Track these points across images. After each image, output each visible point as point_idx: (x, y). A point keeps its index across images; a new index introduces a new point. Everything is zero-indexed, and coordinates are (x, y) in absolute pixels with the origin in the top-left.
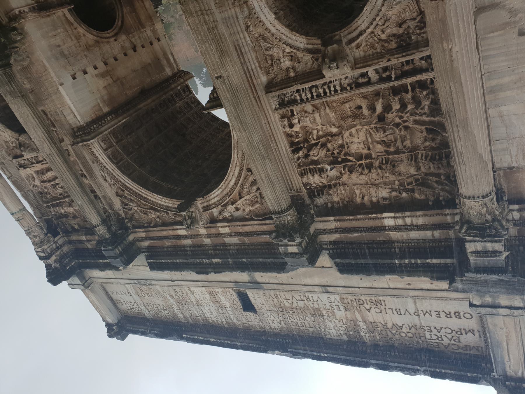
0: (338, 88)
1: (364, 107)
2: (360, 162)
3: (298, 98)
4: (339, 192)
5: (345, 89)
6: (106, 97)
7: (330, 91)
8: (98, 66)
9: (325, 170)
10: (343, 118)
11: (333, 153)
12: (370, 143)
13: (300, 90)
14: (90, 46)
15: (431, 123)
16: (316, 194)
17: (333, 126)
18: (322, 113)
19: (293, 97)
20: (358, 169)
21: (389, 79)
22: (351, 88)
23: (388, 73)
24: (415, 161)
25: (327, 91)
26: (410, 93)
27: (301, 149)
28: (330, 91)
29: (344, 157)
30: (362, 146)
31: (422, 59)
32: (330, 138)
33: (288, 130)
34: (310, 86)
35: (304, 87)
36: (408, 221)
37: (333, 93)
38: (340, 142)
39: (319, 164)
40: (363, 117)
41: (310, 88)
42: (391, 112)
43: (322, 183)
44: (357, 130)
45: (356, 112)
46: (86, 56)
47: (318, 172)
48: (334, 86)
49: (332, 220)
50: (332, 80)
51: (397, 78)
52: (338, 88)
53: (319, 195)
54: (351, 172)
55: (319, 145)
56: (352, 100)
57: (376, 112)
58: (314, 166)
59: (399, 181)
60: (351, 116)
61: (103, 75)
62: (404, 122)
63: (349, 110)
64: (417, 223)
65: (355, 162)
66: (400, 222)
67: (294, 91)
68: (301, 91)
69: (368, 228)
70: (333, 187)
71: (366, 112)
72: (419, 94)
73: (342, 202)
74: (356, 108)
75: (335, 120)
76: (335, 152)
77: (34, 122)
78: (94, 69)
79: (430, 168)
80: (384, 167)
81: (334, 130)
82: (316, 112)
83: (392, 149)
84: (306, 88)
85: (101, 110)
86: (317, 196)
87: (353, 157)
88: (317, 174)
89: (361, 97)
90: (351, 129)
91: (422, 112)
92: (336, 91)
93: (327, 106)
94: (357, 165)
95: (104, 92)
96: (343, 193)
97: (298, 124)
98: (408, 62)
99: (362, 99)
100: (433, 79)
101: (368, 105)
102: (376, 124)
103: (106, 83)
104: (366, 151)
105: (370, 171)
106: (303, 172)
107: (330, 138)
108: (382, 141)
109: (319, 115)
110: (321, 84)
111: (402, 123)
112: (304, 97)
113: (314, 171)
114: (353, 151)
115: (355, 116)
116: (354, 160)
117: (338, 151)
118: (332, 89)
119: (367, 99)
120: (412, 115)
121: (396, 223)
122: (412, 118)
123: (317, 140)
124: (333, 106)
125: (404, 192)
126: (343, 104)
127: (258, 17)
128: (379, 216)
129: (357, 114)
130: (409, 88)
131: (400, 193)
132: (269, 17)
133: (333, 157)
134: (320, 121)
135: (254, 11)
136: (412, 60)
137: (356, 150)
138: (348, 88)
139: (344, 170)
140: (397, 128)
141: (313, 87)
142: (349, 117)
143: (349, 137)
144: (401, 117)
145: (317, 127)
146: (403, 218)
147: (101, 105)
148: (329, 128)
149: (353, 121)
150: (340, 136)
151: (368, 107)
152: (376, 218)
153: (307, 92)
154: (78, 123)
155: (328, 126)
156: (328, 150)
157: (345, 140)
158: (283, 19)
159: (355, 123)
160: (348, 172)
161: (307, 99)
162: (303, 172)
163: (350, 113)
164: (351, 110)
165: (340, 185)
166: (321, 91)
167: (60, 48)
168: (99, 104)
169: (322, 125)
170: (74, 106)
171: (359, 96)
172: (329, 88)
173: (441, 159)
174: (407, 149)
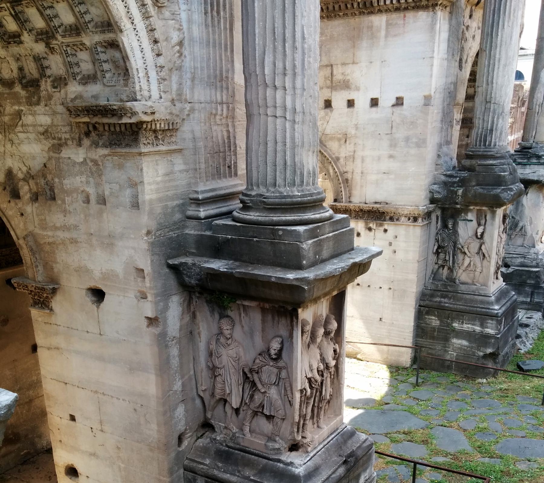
6: (365, 44)
8: (345, 104)
14: (339, 140)
46: (357, 127)
61: (346, 85)
77: (503, 52)
78: (356, 102)
85: (388, 24)
95: (363, 54)
103: (348, 69)
127: (158, 55)
132: (135, 44)
135: (163, 74)
147: (383, 33)
154: (442, 18)
158: (92, 24)
167: (391, 152)
168: (386, 36)
170: (433, 51)
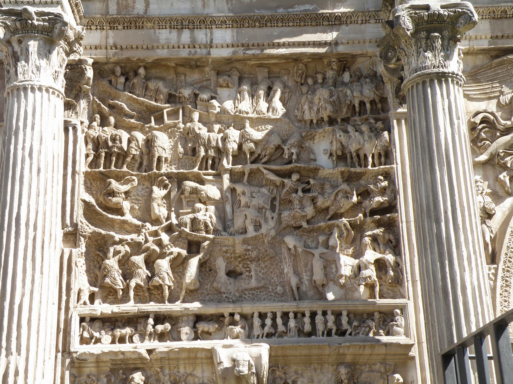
0: (257, 322)
1: (222, 273)
2: (254, 166)
3: (344, 320)
4: (315, 109)
5: (243, 316)
7: (274, 319)
9: (334, 158)
10: (269, 259)
11: (304, 191)
12: (230, 201)
13: (336, 334)
15: (110, 225)
16: (368, 106)
17: (291, 246)
18: (308, 278)
19: (355, 323)
20: (263, 154)
21: (159, 319)
22: (232, 315)
23: (160, 328)
24: (153, 156)
25: (279, 321)
26: (133, 284)
27: (373, 212)
28: (274, 319)
29: (286, 181)
30: (244, 200)
31: (98, 341)
32: (305, 225)
33: (390, 258)
34: (313, 337)
35: (325, 337)
36: (186, 36)
37: (269, 315)
38: (285, 214)
39: (342, 173)
40: (228, 255)
41: (313, 333)
42: (172, 256)
43: (346, 132)
44: (246, 232)
45: (240, 265)
47: (348, 156)
48: (263, 326)
49: (342, 43)
50: (264, 337)
51: (146, 316)
52: (257, 322)
53: (362, 104)
54: (279, 148)
55: (331, 213)
56: (242, 291)
57: (200, 260)
58: (353, 170)
59: (192, 121)
60: (251, 261)
62: (155, 234)
63: (253, 273)
64: (170, 32)
65: (265, 168)
66: (201, 36)
67: (350, 334)
68: (334, 331)
69: (269, 24)
70: (326, 119)
71: (221, 265)
72: (118, 278)
73: (315, 82)
74: (241, 274)
75: (285, 258)
76: (300, 193)
79: (129, 141)
80: (212, 153)
81: (290, 241)
82: (318, 283)
83: (190, 184)
84: (323, 334)
86: (366, 100)
87: (267, 179)
88: (351, 152)
89: (224, 293)
90: (255, 237)
91: (119, 247)
92: (262, 316)
93: (295, 289)
94: (263, 160)
96: (307, 104)
97: (362, 265)
98: (122, 340)
99: (223, 290)
100: (88, 302)
101: (215, 277)
102: (206, 239)
104: (239, 189)
105: (240, 146)
106: (383, 159)
107: (305, 225)
108: (204, 203)
109: (313, 275)
110: (289, 335)
111: (160, 231)
112: (331, 318)
113: (355, 159)
114: (264, 190)
115: (243, 260)
116: (265, 171)
117: (294, 195)
118: (268, 322)
119: (213, 287)
120: (139, 244)
121: (209, 35)
122: (141, 239)
123: (334, 224)
124: (283, 286)
125: (186, 95)
126: (262, 287)
128: (241, 53)
129: (240, 262)
130: (132, 293)
131: (196, 95)
133: (308, 183)
134: (314, 262)
136: (113, 342)
137: (259, 192)
138: (237, 317)
139: (293, 153)
140: (171, 224)
141: (309, 334)
142: (257, 259)
143: (262, 221)
144: (159, 243)
145: (325, 251)
146: (193, 45)
148: (298, 245)
149: (249, 250)
150: (284, 225)
151: (216, 272)
152: (247, 47)
153: (320, 327)
155: (300, 250)
156: (313, 200)
157: (275, 215)
159: (245, 247)
160: (285, 148)
161: (324, 313)
162: (383, 159)
163: (253, 266)
164: (250, 271)
165: (312, 121)
166: (292, 323)
169: (314, 255)
171: (228, 295)
172: (274, 325)
173: (108, 156)
174: (163, 181)
